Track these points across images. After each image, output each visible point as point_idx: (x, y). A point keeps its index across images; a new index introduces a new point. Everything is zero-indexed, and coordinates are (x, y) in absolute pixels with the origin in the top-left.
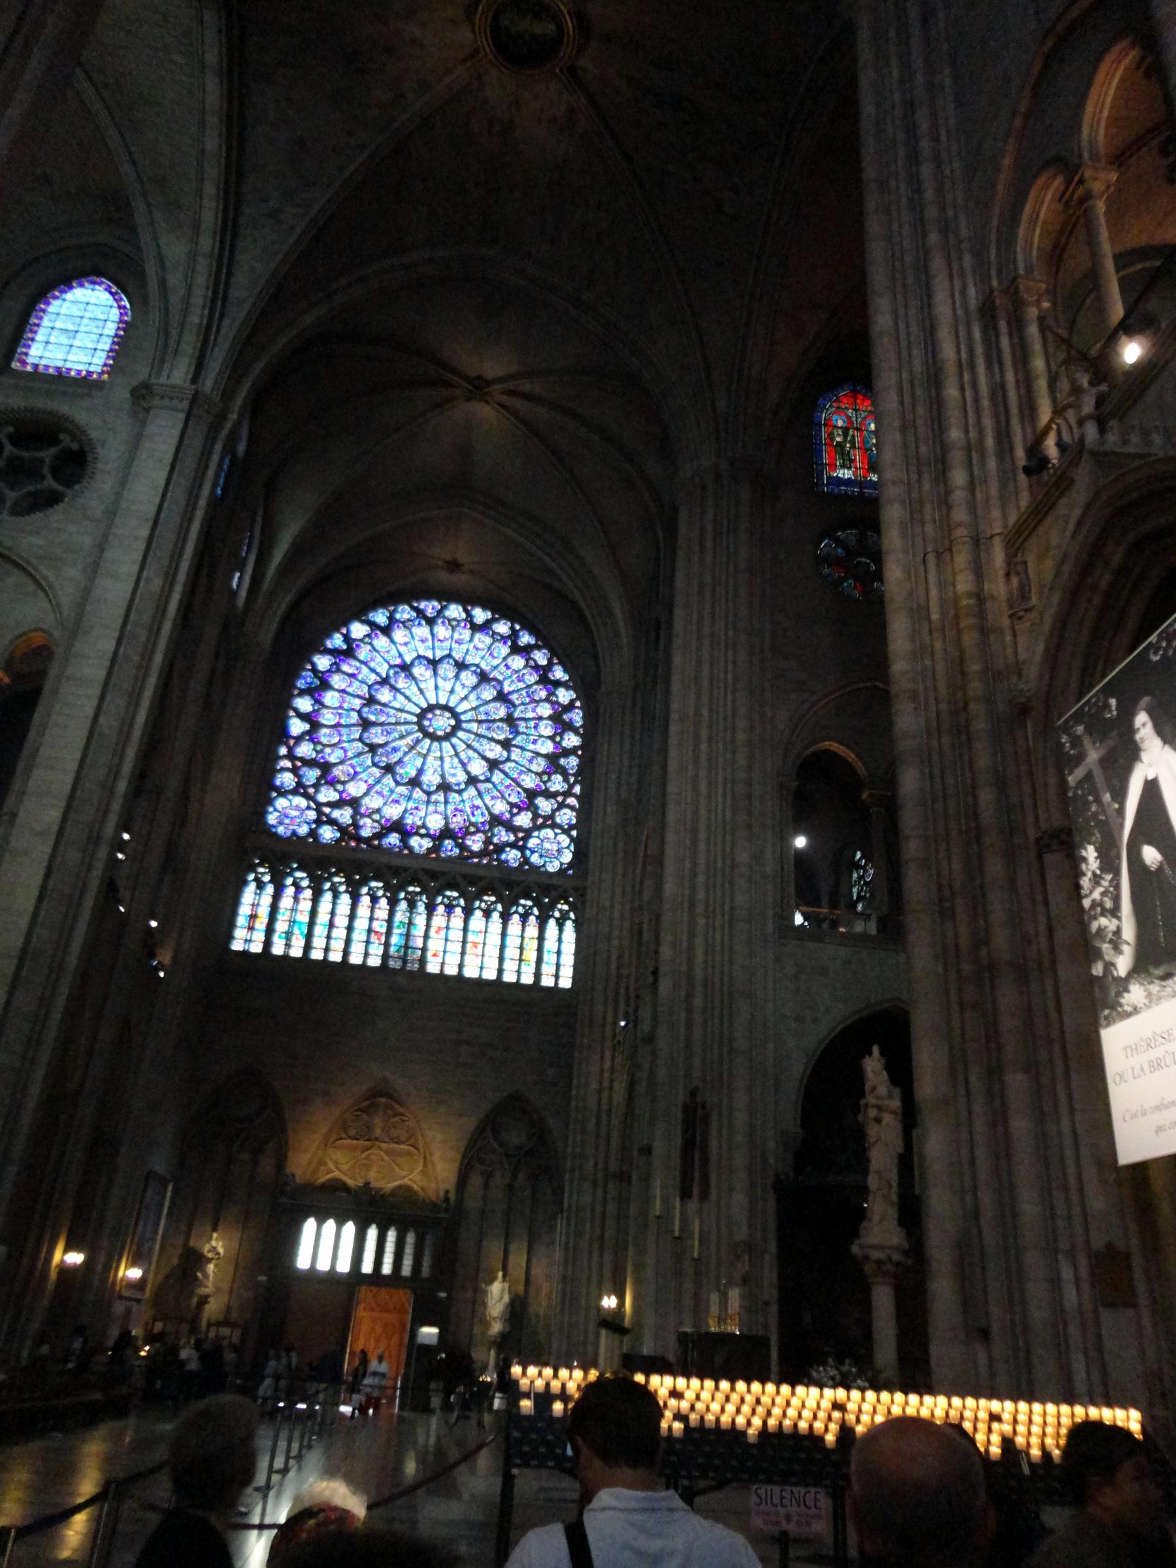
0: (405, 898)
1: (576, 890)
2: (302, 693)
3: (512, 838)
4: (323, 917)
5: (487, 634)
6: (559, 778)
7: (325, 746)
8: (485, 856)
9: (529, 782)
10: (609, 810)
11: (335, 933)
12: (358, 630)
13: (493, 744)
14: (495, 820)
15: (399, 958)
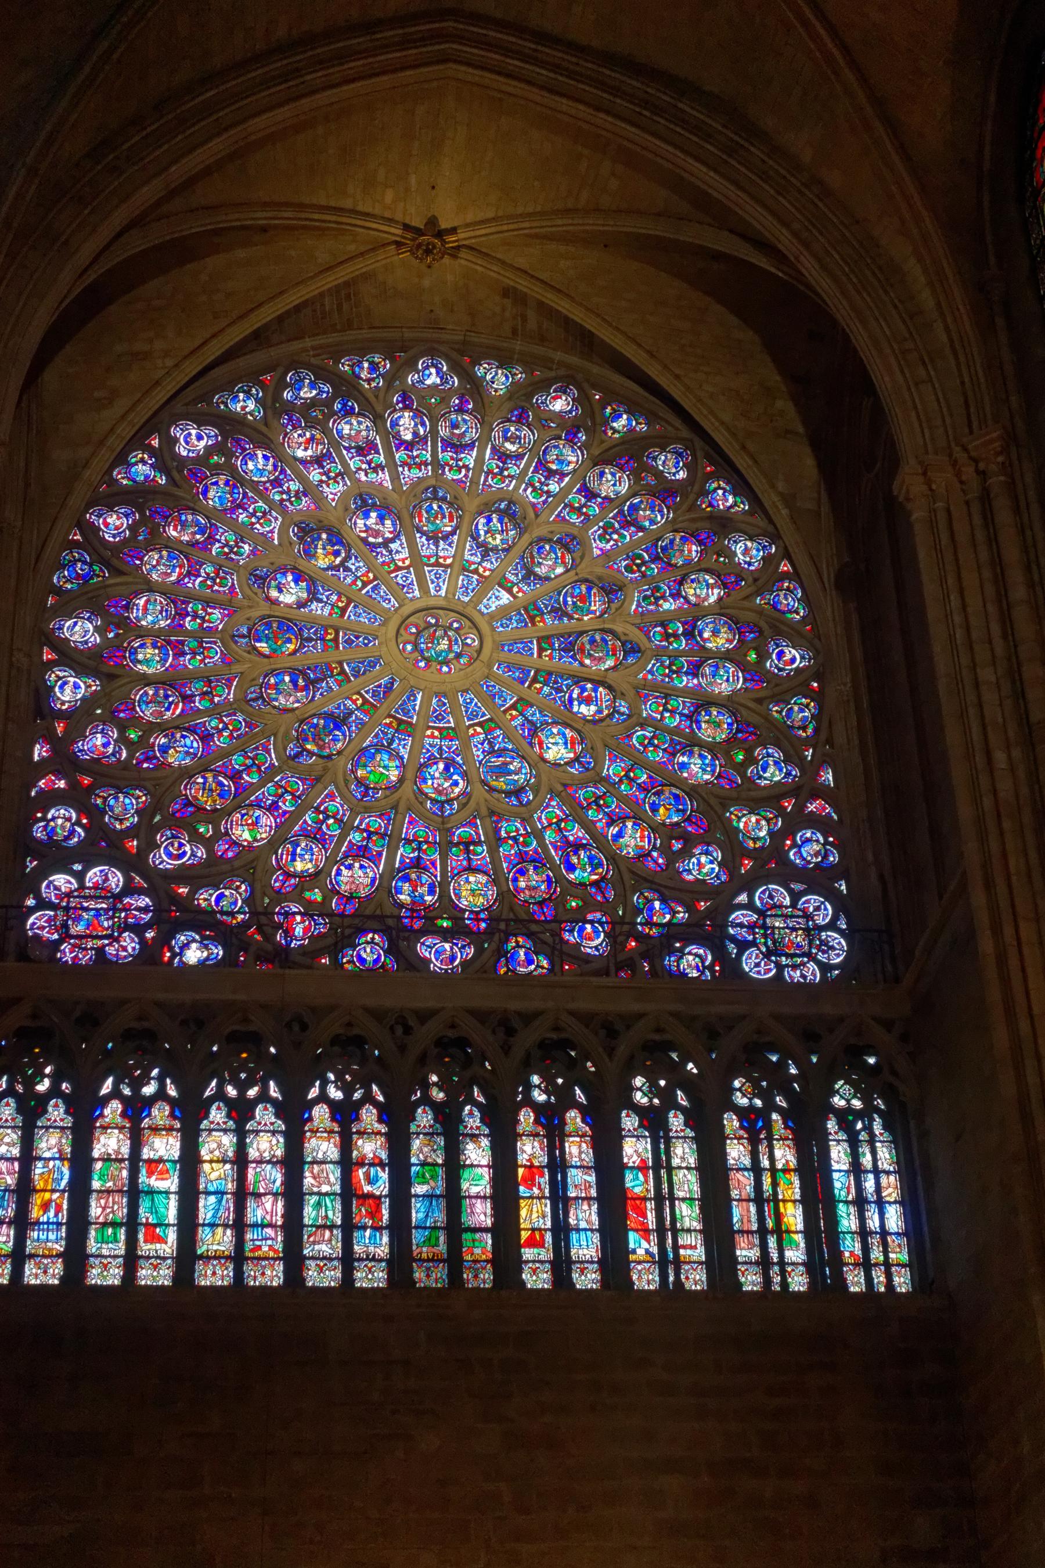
0: (426, 1100)
1: (888, 1025)
2: (70, 605)
3: (682, 915)
4: (215, 1174)
5: (521, 419)
6: (778, 755)
7: (150, 728)
8: (619, 968)
9: (697, 769)
10: (1000, 758)
11: (255, 1213)
12: (192, 441)
13: (589, 686)
14: (630, 875)
15: (434, 1259)
